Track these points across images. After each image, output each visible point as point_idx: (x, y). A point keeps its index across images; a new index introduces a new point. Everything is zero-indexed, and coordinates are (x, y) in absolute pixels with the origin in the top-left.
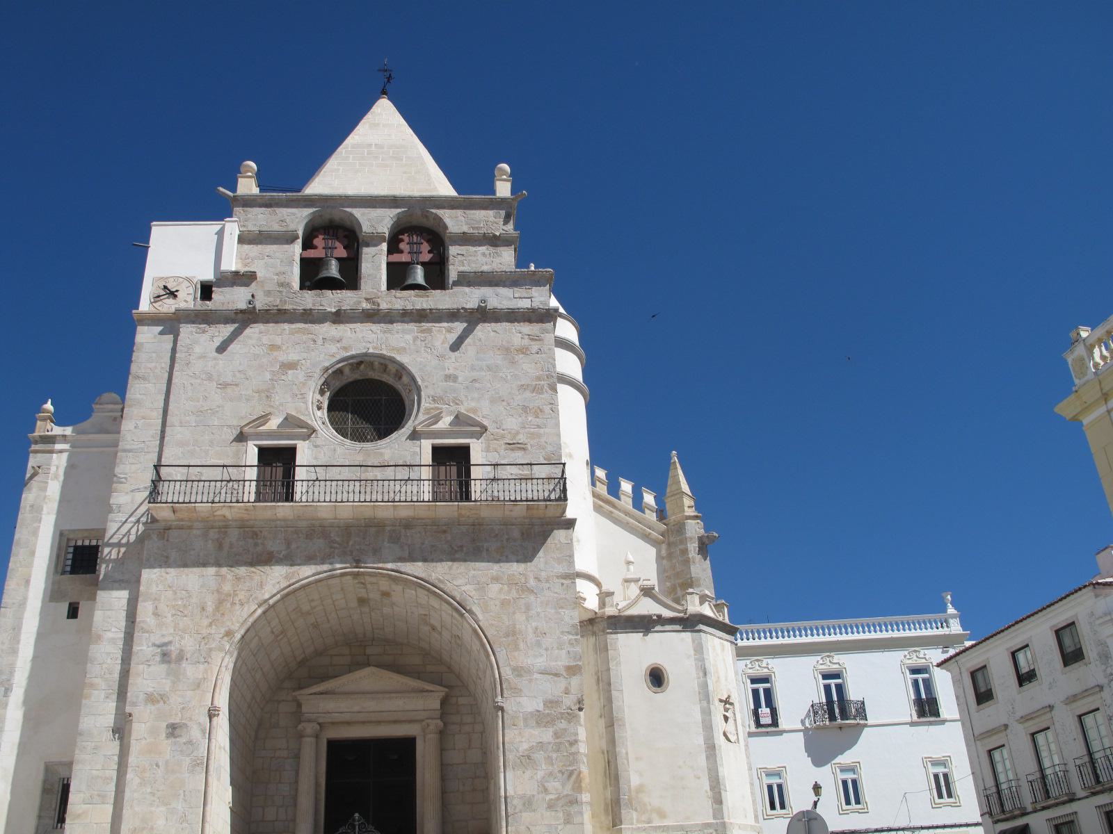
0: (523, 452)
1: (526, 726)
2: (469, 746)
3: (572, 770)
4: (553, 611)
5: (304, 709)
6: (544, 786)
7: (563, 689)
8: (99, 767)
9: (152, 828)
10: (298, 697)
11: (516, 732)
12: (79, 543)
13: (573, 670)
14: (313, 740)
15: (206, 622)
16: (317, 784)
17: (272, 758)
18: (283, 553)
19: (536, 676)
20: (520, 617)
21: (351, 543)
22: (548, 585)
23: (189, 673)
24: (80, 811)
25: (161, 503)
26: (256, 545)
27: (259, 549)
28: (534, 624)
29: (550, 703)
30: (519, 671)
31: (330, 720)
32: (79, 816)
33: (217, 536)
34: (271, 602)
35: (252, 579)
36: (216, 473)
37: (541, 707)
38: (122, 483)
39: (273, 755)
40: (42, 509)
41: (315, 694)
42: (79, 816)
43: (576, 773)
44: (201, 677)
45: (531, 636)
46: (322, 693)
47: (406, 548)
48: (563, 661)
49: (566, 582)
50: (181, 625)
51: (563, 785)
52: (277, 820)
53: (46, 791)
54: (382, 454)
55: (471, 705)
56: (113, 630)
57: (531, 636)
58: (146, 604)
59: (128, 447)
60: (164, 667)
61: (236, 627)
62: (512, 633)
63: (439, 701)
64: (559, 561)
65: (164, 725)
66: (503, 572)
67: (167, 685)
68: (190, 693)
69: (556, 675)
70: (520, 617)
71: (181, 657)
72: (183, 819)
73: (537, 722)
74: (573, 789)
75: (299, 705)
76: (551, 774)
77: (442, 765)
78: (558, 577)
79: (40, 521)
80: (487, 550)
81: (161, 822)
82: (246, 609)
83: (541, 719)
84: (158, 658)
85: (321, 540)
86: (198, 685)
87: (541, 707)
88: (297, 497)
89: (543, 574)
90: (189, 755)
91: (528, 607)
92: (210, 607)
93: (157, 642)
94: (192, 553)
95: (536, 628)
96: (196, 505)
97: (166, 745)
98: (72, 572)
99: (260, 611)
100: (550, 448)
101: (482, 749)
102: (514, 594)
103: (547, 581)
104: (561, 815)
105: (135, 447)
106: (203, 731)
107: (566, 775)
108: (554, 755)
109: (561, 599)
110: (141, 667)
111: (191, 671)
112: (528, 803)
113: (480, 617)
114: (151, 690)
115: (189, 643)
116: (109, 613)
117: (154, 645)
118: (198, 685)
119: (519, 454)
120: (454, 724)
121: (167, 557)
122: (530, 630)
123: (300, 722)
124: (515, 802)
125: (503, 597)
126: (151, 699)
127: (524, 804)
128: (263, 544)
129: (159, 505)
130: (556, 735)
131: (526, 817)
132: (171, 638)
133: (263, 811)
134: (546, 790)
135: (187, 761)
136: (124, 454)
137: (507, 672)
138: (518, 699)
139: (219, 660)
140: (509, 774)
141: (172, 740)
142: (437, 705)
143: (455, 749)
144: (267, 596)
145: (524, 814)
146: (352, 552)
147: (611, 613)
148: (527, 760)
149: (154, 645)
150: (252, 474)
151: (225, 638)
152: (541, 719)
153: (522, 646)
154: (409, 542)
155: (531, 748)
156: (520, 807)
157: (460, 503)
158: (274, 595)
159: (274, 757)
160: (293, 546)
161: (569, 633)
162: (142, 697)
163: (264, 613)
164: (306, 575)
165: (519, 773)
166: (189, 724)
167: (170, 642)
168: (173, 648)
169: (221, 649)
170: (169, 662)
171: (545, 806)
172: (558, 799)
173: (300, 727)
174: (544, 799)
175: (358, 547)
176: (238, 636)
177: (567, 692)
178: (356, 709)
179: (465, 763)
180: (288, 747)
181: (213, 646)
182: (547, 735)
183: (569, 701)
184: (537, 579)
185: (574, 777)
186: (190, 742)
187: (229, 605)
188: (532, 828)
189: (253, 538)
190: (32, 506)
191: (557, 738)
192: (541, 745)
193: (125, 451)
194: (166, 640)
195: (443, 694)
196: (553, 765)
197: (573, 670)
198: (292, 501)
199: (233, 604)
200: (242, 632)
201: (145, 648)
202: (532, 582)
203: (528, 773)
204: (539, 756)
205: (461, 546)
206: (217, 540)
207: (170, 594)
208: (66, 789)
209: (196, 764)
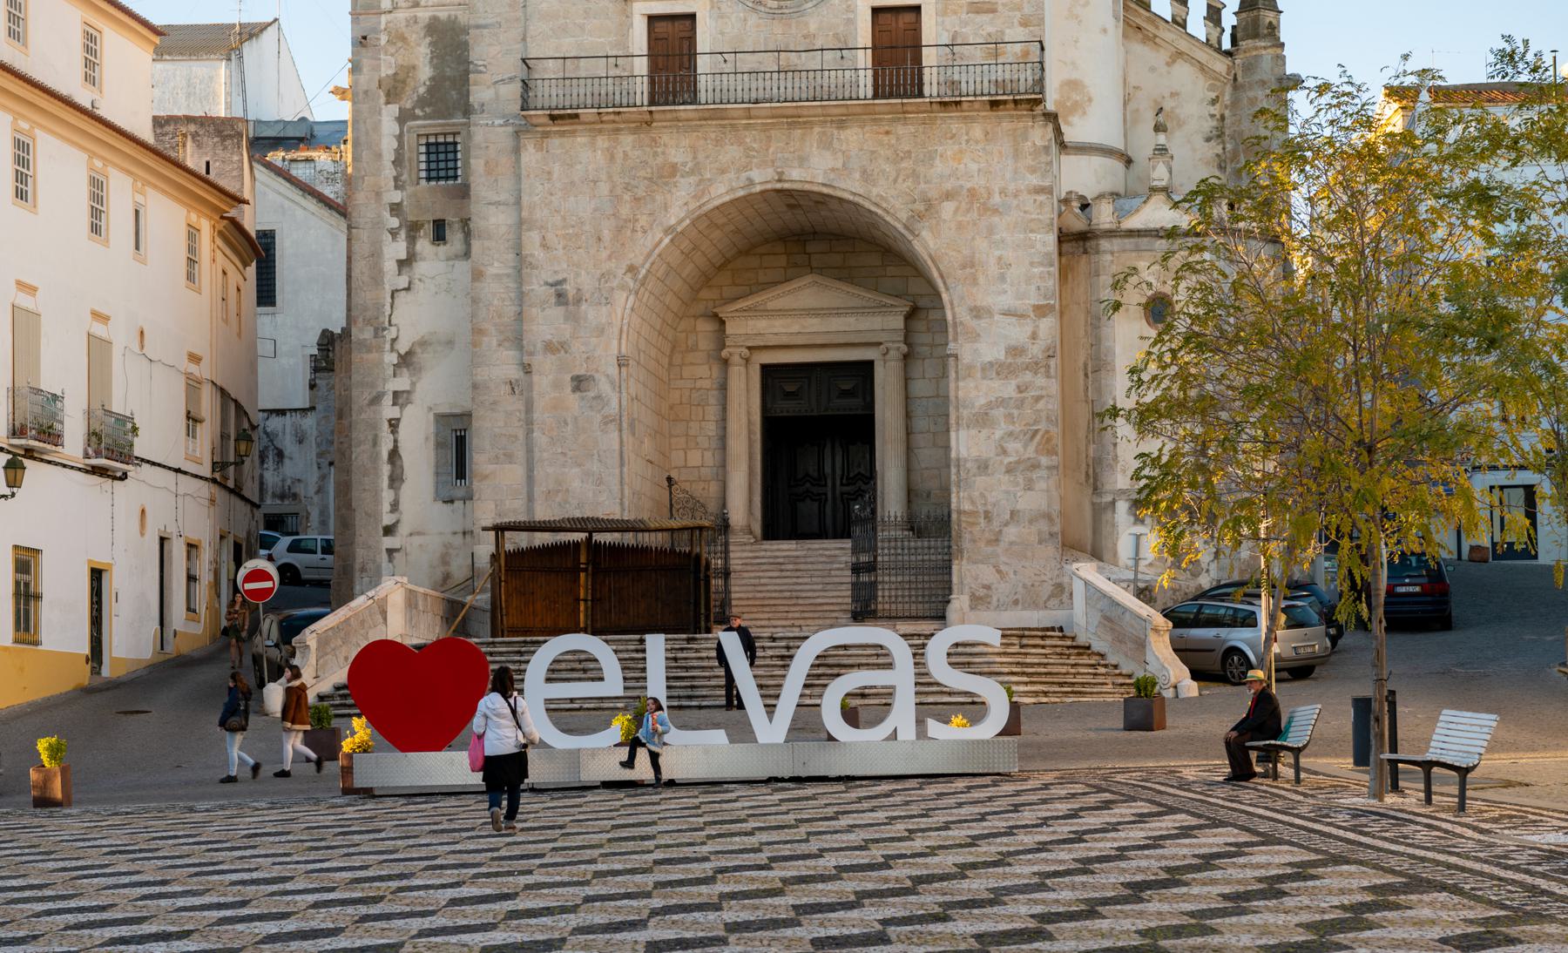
0: (991, 15)
1: (984, 378)
3: (1037, 431)
4: (1022, 236)
5: (729, 330)
6: (1002, 447)
7: (1029, 333)
8: (501, 424)
9: (567, 490)
11: (972, 385)
12: (432, 140)
13: (1041, 311)
14: (743, 369)
15: (604, 254)
16: (749, 422)
18: (690, 165)
19: (997, 317)
20: (981, 244)
21: (771, 150)
22: (1015, 202)
23: (591, 317)
24: (488, 472)
25: (536, 109)
26: (655, 154)
27: (660, 160)
28: (997, 253)
29: (1015, 351)
30: (977, 312)
31: (762, 344)
32: (486, 477)
33: (606, 145)
34: (679, 229)
35: (654, 200)
36: (599, 68)
37: (1002, 358)
38: (481, 72)
40: (379, 96)
42: (486, 477)
43: (1041, 433)
44: (604, 321)
45: (993, 270)
46: (749, 309)
47: (840, 154)
48: (1034, 299)
49: (1042, 198)
50: (575, 258)
51: (1025, 446)
53: (439, 445)
54: (806, 24)
56: (496, 264)
57: (993, 270)
58: (531, 234)
59: (482, 22)
60: (561, 309)
61: (638, 261)
62: (970, 263)
64: (1033, 170)
65: (568, 377)
66: (962, 186)
67: (566, 330)
68: (594, 340)
69: (1022, 316)
70: (981, 244)
71: (578, 301)
72: (600, 481)
73: (998, 374)
74: (1037, 451)
75: (722, 323)
76: (1011, 434)
77: (907, 398)
78: (1029, 192)
79: (380, 114)
80: (941, 156)
81: (576, 484)
82: (649, 237)
83: (1001, 370)
84: (553, 300)
85: (735, 147)
86: (601, 331)
87: (1002, 358)
88: (702, 96)
89: (1012, 187)
90: (599, 411)
91: (991, 230)
92: (607, 234)
93: (550, 281)
94: (579, 167)
95: (1000, 258)
96: (579, 111)
97: (573, 400)
98: (429, 179)
99: (667, 240)
100: (1027, 10)
102: (975, 215)
103: (1016, 196)
104: (1020, 480)
105: (489, 21)
106: (612, 383)
107: (1028, 436)
108: (1016, 412)
109: (1032, 220)
110: (534, 310)
111: (592, 314)
112: (984, 467)
113: (931, 244)
114: (549, 337)
115: (583, 280)
116: (487, 243)
117: (547, 283)
118: (601, 331)
119: (985, 18)
120: (923, 345)
121: (549, 173)
122: (992, 261)
123: (723, 346)
124: (969, 465)
125: (960, 218)
126: (550, 348)
127: (979, 468)
128: (663, 153)
129: (532, 112)
130: (1020, 389)
131: (980, 482)
132: (565, 275)
134: (1004, 452)
135: (599, 417)
136: (478, 31)
137: (963, 315)
138: (977, 345)
139: (623, 300)
140: (963, 433)
141: (578, 394)
142: (897, 322)
144: (673, 221)
145: (978, 478)
146: (773, 162)
147: (1107, 226)
148: (982, 420)
149: (547, 283)
150: (641, 66)
151: (629, 275)
152: (1001, 370)
153: (981, 280)
154: (844, 148)
155: (990, 405)
156: (974, 470)
157: (905, 101)
158: (682, 220)
160: (701, 156)
161: (1041, 264)
162: (539, 346)
163: (672, 240)
164: (719, 192)
165: (973, 432)
166: (597, 376)
167: (564, 281)
168: (568, 287)
169: (623, 287)
170: (566, 304)
171: (1004, 470)
172: (1018, 462)
173: (724, 353)
174: (1001, 462)
175: (779, 155)
176: (643, 271)
177: (1034, 336)
178: (795, 328)
179: (938, 396)
181: (615, 284)
182: (1009, 389)
183: (1036, 350)
184: (1003, 192)
185: (1038, 437)
186: (598, 397)
187: (629, 233)
188: (986, 494)
189: (652, 147)
190: (366, 92)
191: (1021, 392)
192: (1002, 402)
193: (478, 27)
194: (560, 277)
196: (1014, 423)
197: (1041, 311)
198: (694, 101)
199: (634, 231)
200: (647, 265)
201: (535, 287)
202: (996, 199)
203: (985, 432)
204: (998, 413)
205: (909, 152)
206: (608, 149)
207: (557, 220)
208: (461, 444)
209: (607, 421)
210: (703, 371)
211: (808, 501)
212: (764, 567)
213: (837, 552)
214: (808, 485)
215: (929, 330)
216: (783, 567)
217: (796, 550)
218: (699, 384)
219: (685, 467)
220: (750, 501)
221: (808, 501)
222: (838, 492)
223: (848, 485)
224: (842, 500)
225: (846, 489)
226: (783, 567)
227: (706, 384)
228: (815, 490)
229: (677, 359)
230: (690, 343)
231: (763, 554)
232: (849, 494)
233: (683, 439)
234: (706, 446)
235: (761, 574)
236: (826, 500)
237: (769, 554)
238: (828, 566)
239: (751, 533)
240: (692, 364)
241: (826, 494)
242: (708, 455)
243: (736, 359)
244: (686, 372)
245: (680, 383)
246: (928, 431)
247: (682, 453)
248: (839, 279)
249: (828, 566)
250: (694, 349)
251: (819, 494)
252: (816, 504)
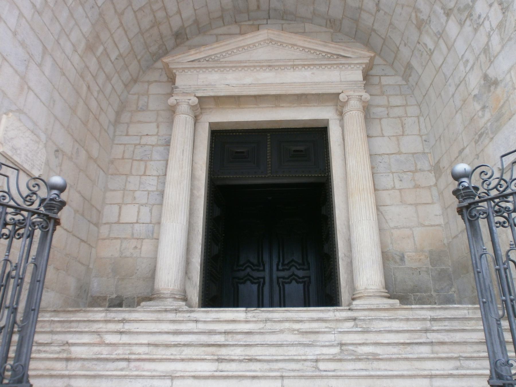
2: (403, 132)
5: (179, 81)
10: (171, 66)
16: (193, 177)
17: (136, 145)
39: (138, 142)
41: (192, 61)
52: (137, 223)
55: (400, 85)
63: (361, 72)
101: (421, 136)
120: (378, 106)
133: (120, 208)
143: (383, 136)
159: (139, 144)
173: (172, 101)
178: (248, 80)
179: (400, 153)
180: (158, 132)
195: (367, 61)
210: (151, 128)
211: (248, 283)
212: (188, 352)
213: (315, 326)
214: (249, 270)
215: (382, 94)
216: (224, 352)
217: (247, 322)
218: (144, 141)
219: (118, 223)
220: (188, 262)
221: (248, 283)
222: (275, 277)
223: (283, 270)
224: (278, 283)
225: (281, 274)
226: (224, 352)
227: (153, 140)
228: (256, 274)
229: (125, 117)
230: (140, 105)
231: (191, 326)
232: (283, 278)
233: (119, 194)
234: (144, 201)
235: (179, 366)
236: (264, 283)
237: (201, 327)
238: (311, 353)
239: (185, 299)
240: (140, 122)
241: (264, 278)
242: (145, 210)
243: (184, 107)
244: (133, 130)
245: (125, 140)
246: (394, 188)
247: (116, 208)
248: (296, 33)
249: (311, 353)
250: (145, 109)
251: (258, 278)
252: (255, 287)
